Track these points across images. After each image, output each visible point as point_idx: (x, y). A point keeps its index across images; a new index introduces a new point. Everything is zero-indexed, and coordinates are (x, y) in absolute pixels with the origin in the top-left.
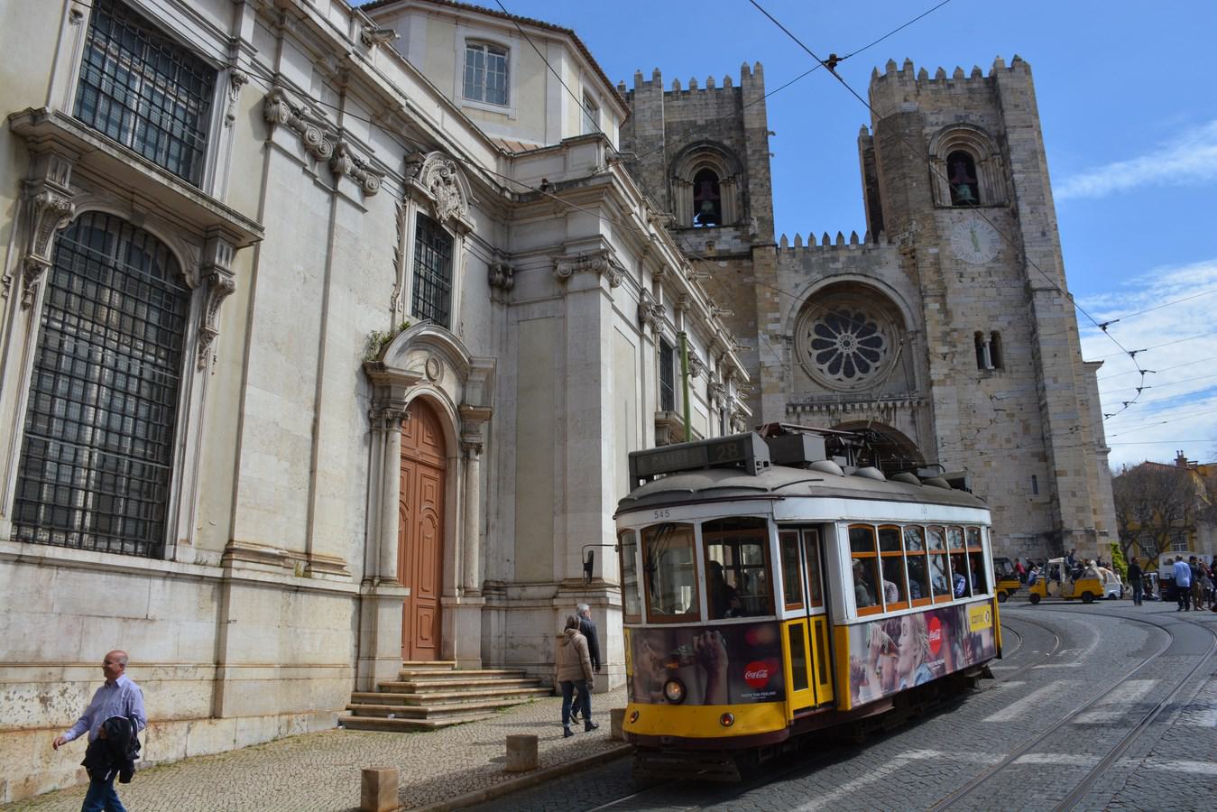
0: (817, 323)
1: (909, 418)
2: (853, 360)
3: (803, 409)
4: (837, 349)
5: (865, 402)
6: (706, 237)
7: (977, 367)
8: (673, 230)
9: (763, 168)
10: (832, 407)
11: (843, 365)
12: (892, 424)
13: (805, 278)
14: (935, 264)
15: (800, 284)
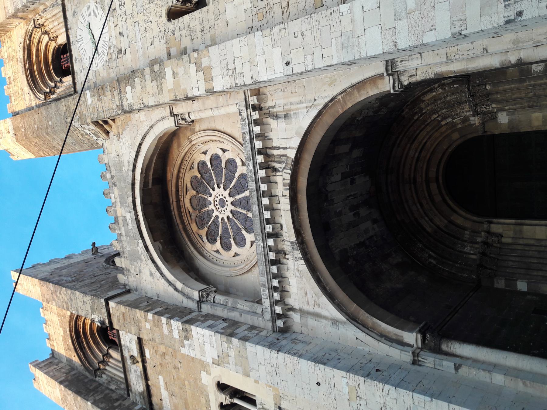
0: (205, 239)
1: (281, 123)
2: (238, 197)
3: (277, 302)
4: (228, 218)
5: (259, 202)
6: (129, 361)
7: (204, 9)
8: (129, 395)
9: (60, 294)
10: (272, 256)
11: (244, 212)
12: (292, 154)
13: (144, 262)
14: (99, 93)
15: (149, 269)
